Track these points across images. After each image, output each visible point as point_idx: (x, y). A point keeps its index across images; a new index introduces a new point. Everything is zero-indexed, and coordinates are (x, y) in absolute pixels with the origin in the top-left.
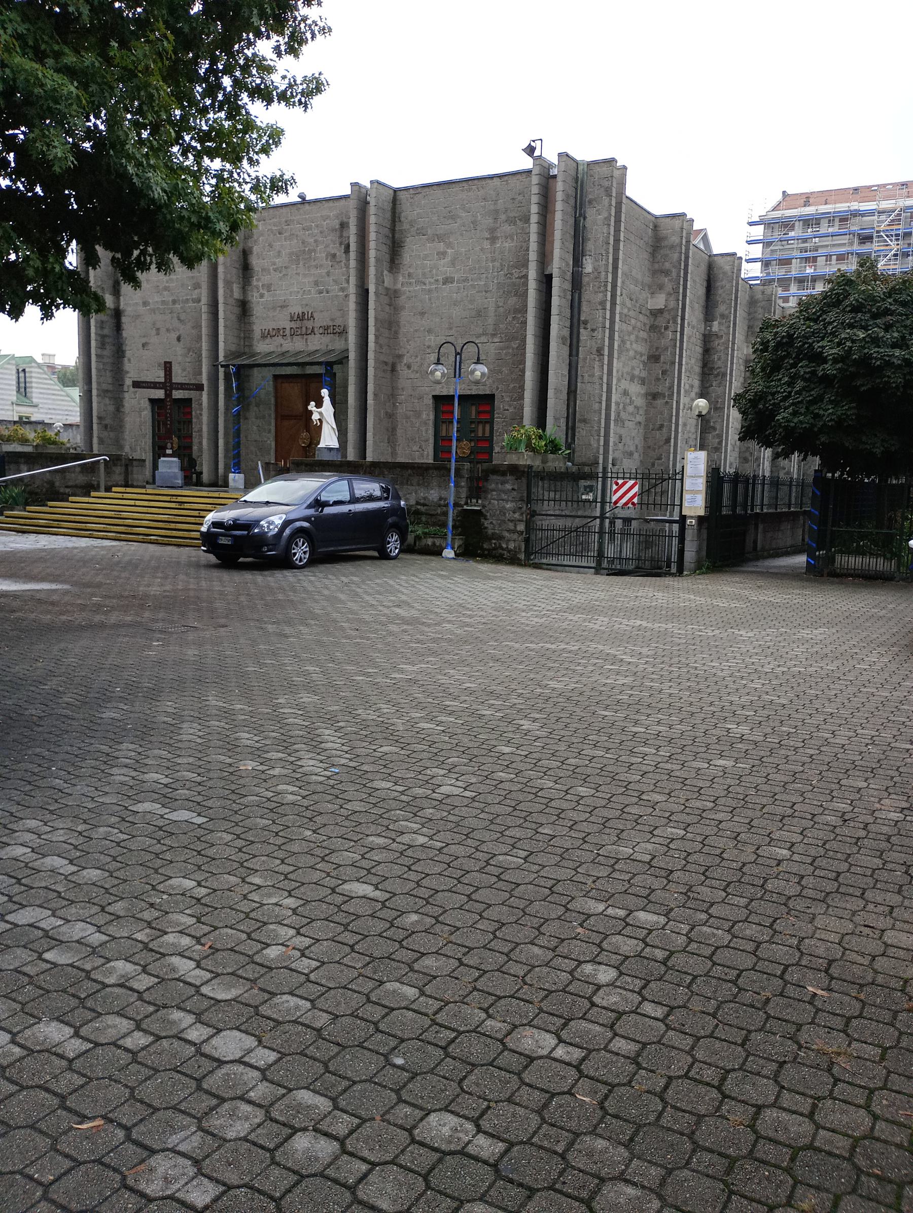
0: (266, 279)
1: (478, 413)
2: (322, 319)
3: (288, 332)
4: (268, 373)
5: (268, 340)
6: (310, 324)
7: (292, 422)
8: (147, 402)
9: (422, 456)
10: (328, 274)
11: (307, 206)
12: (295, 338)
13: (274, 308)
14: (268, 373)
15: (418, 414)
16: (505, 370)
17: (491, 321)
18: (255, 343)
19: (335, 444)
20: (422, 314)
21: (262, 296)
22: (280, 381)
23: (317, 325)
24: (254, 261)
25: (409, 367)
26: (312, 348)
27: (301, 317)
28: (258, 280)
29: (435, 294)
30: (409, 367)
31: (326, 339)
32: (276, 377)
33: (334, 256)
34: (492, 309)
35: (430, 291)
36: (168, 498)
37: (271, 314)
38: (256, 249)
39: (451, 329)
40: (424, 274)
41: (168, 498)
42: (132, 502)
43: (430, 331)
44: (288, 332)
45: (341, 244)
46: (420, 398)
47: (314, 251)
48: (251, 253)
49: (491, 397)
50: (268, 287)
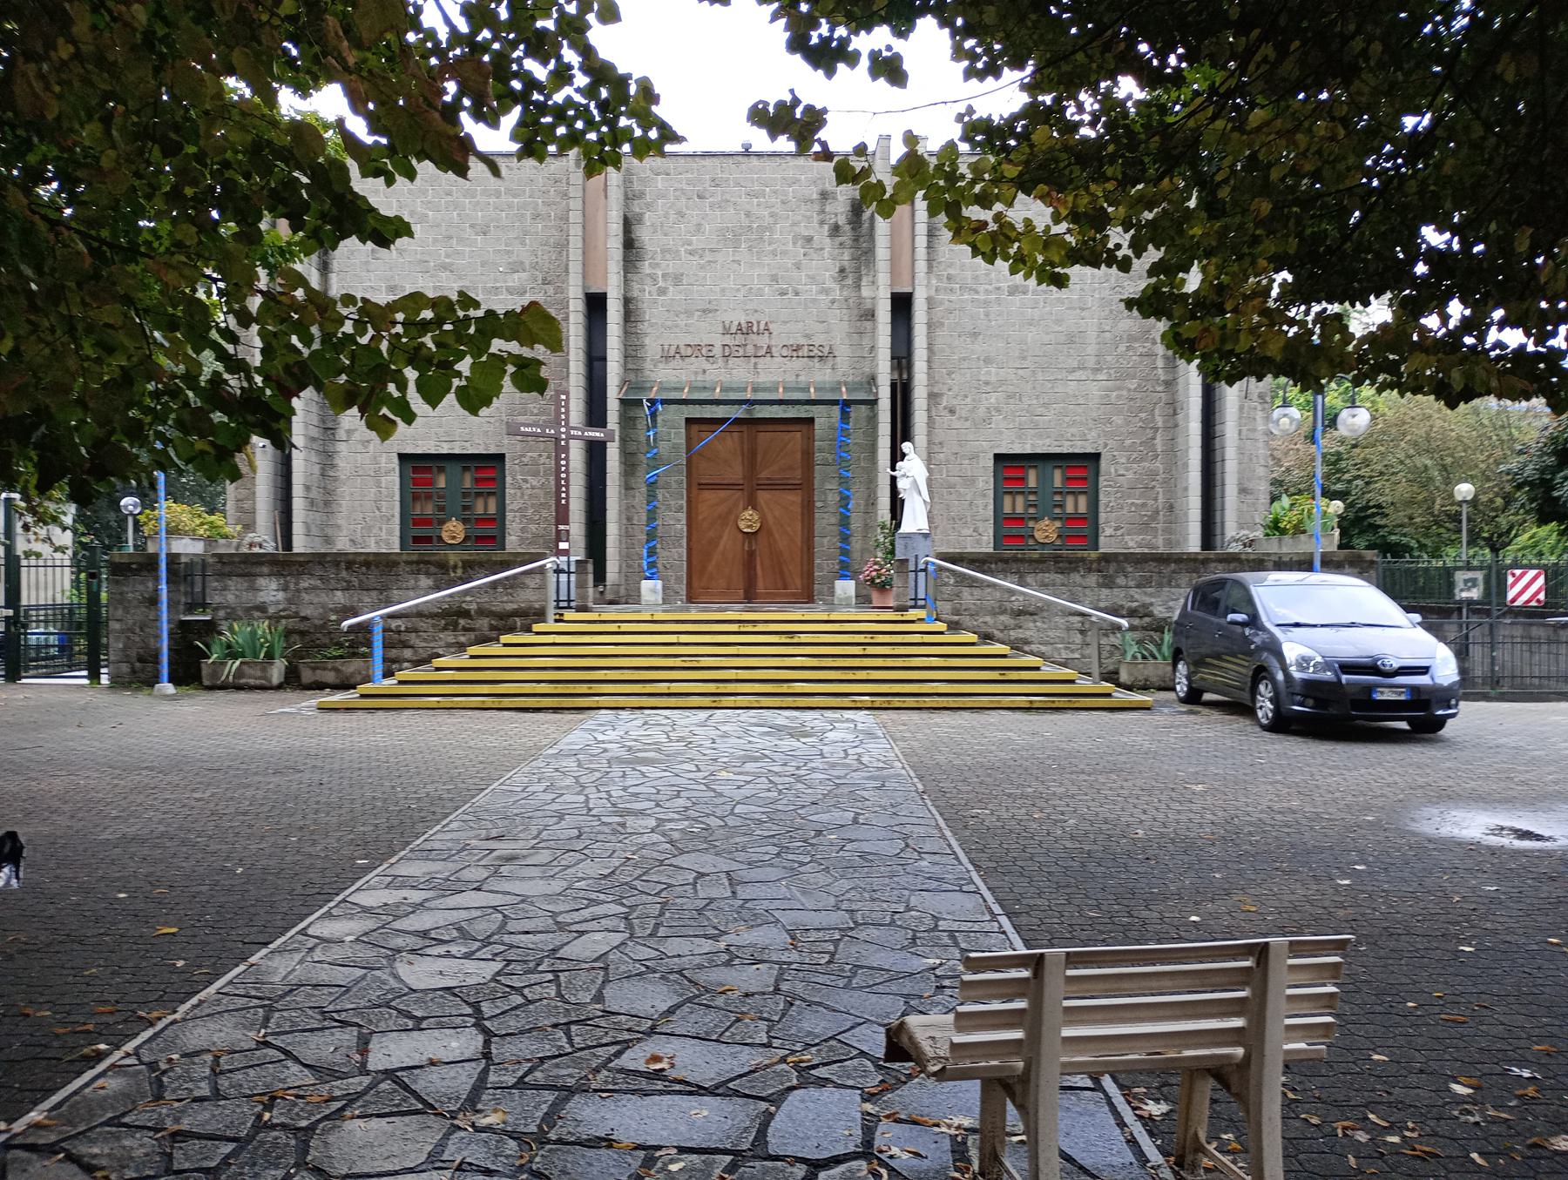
0: (671, 266)
1: (477, 481)
2: (782, 335)
3: (717, 351)
4: (677, 415)
5: (677, 362)
6: (763, 341)
7: (723, 494)
8: (396, 460)
9: (978, 542)
10: (798, 267)
11: (754, 161)
12: (732, 361)
13: (689, 314)
14: (677, 415)
15: (970, 481)
16: (1118, 420)
17: (1091, 349)
18: (648, 365)
19: (923, 525)
20: (975, 335)
21: (662, 291)
22: (695, 428)
23: (777, 342)
24: (643, 234)
25: (952, 412)
26: (764, 378)
27: (746, 330)
28: (655, 266)
29: (994, 308)
30: (952, 412)
31: (797, 364)
32: (688, 421)
33: (809, 240)
34: (1092, 335)
35: (986, 303)
36: (734, 627)
37: (682, 321)
38: (648, 217)
39: (1024, 358)
40: (976, 278)
41: (734, 627)
42: (673, 638)
43: (988, 361)
44: (717, 351)
45: (822, 223)
46: (974, 457)
47: (770, 229)
48: (640, 221)
49: (1096, 457)
50: (677, 279)
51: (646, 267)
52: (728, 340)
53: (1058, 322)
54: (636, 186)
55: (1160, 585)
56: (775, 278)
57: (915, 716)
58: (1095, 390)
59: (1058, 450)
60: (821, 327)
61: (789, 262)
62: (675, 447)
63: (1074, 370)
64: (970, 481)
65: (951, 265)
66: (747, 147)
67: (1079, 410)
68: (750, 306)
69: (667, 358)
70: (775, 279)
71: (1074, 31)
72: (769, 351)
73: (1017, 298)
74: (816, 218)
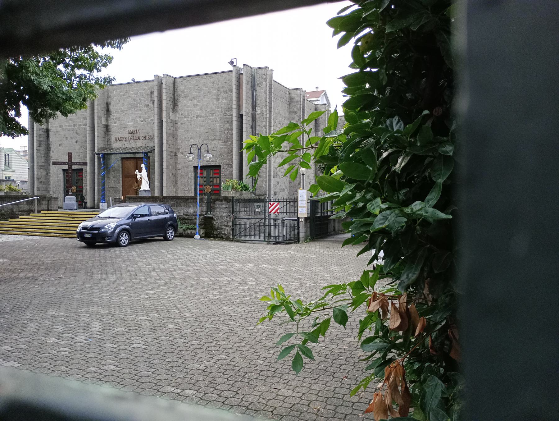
0: (117, 115)
2: (142, 133)
3: (127, 139)
4: (119, 157)
5: (118, 142)
6: (137, 135)
7: (130, 179)
8: (61, 171)
9: (189, 192)
10: (145, 113)
11: (135, 84)
12: (131, 141)
13: (121, 128)
14: (119, 157)
15: (187, 174)
16: (225, 155)
17: (218, 134)
18: (112, 143)
19: (148, 188)
20: (188, 130)
21: (115, 123)
22: (124, 160)
23: (141, 135)
24: (111, 107)
25: (182, 154)
26: (138, 146)
27: (134, 132)
28: (114, 116)
29: (193, 122)
30: (182, 154)
31: (146, 141)
32: (122, 159)
33: (148, 105)
34: (218, 129)
35: (191, 121)
36: (67, 216)
37: (120, 131)
38: (112, 103)
39: (200, 137)
40: (188, 114)
41: (67, 216)
42: (50, 218)
43: (191, 138)
44: (127, 139)
45: (151, 100)
46: (188, 167)
47: (139, 103)
48: (110, 104)
49: (219, 167)
50: (118, 119)
51: (112, 116)
52: (130, 135)
53: (209, 125)
54: (110, 94)
55: (177, 206)
56: (140, 117)
57: (68, 239)
58: (219, 145)
59: (209, 165)
60: (151, 130)
61: (143, 112)
62: (118, 166)
63: (213, 140)
64: (187, 174)
65: (182, 110)
66: (133, 80)
67: (215, 152)
68: (135, 125)
69: (116, 141)
70: (140, 117)
71: (393, 7)
72: (139, 138)
73: (199, 119)
74: (150, 99)
